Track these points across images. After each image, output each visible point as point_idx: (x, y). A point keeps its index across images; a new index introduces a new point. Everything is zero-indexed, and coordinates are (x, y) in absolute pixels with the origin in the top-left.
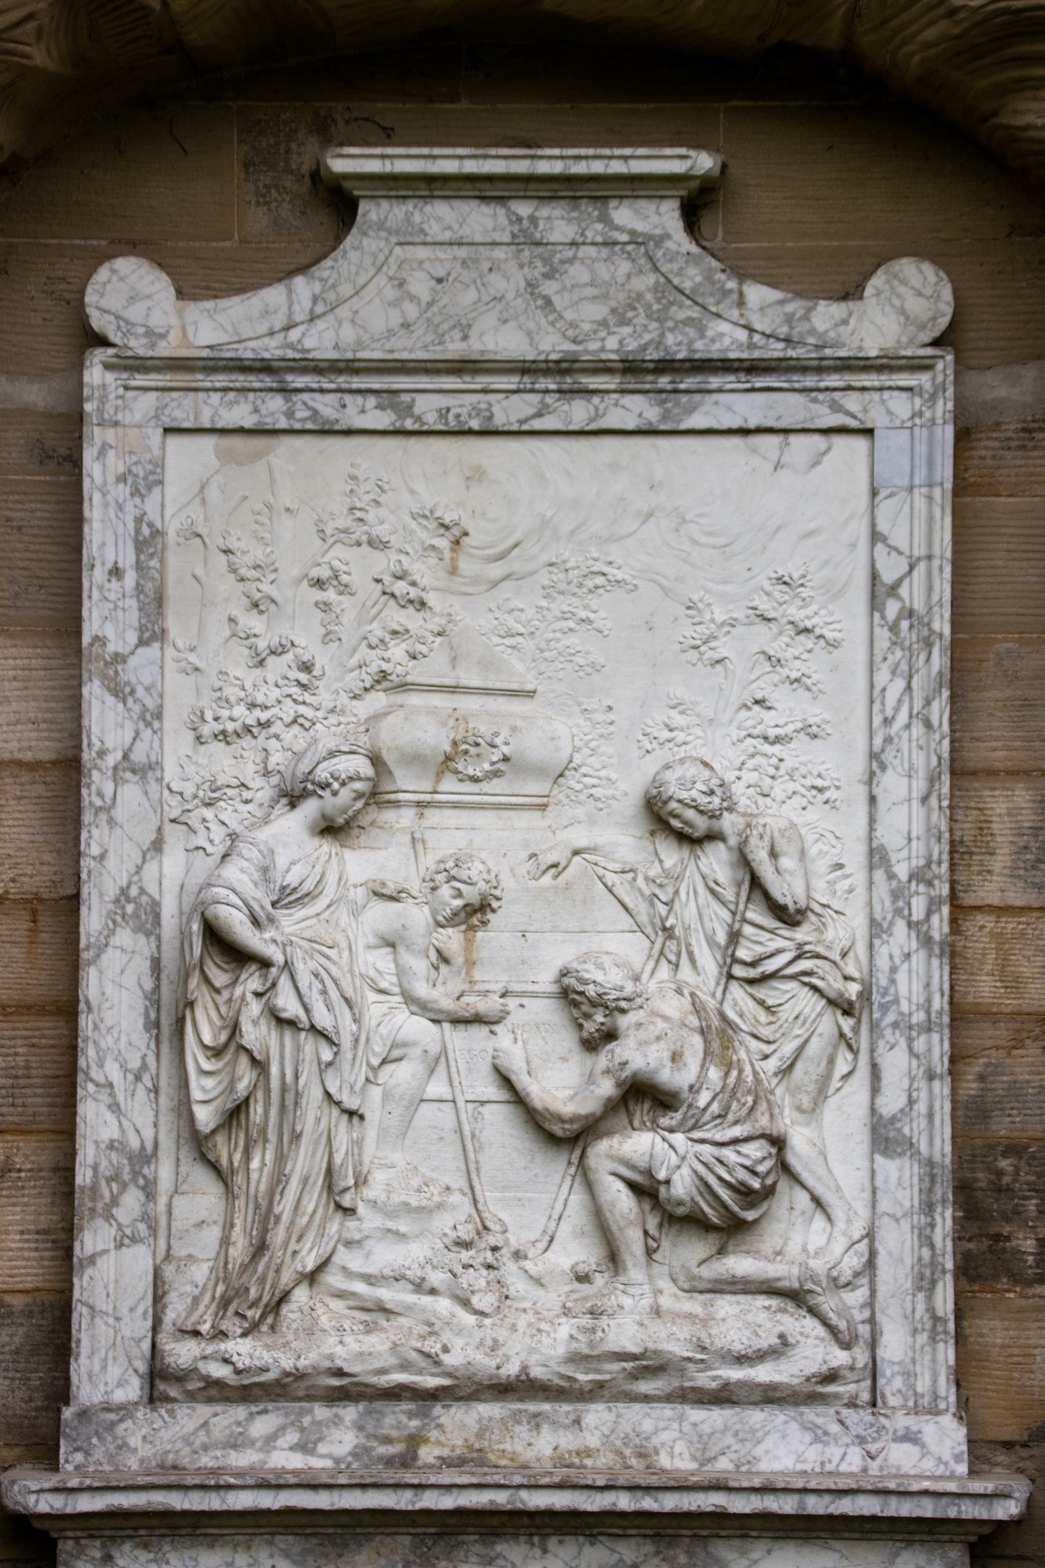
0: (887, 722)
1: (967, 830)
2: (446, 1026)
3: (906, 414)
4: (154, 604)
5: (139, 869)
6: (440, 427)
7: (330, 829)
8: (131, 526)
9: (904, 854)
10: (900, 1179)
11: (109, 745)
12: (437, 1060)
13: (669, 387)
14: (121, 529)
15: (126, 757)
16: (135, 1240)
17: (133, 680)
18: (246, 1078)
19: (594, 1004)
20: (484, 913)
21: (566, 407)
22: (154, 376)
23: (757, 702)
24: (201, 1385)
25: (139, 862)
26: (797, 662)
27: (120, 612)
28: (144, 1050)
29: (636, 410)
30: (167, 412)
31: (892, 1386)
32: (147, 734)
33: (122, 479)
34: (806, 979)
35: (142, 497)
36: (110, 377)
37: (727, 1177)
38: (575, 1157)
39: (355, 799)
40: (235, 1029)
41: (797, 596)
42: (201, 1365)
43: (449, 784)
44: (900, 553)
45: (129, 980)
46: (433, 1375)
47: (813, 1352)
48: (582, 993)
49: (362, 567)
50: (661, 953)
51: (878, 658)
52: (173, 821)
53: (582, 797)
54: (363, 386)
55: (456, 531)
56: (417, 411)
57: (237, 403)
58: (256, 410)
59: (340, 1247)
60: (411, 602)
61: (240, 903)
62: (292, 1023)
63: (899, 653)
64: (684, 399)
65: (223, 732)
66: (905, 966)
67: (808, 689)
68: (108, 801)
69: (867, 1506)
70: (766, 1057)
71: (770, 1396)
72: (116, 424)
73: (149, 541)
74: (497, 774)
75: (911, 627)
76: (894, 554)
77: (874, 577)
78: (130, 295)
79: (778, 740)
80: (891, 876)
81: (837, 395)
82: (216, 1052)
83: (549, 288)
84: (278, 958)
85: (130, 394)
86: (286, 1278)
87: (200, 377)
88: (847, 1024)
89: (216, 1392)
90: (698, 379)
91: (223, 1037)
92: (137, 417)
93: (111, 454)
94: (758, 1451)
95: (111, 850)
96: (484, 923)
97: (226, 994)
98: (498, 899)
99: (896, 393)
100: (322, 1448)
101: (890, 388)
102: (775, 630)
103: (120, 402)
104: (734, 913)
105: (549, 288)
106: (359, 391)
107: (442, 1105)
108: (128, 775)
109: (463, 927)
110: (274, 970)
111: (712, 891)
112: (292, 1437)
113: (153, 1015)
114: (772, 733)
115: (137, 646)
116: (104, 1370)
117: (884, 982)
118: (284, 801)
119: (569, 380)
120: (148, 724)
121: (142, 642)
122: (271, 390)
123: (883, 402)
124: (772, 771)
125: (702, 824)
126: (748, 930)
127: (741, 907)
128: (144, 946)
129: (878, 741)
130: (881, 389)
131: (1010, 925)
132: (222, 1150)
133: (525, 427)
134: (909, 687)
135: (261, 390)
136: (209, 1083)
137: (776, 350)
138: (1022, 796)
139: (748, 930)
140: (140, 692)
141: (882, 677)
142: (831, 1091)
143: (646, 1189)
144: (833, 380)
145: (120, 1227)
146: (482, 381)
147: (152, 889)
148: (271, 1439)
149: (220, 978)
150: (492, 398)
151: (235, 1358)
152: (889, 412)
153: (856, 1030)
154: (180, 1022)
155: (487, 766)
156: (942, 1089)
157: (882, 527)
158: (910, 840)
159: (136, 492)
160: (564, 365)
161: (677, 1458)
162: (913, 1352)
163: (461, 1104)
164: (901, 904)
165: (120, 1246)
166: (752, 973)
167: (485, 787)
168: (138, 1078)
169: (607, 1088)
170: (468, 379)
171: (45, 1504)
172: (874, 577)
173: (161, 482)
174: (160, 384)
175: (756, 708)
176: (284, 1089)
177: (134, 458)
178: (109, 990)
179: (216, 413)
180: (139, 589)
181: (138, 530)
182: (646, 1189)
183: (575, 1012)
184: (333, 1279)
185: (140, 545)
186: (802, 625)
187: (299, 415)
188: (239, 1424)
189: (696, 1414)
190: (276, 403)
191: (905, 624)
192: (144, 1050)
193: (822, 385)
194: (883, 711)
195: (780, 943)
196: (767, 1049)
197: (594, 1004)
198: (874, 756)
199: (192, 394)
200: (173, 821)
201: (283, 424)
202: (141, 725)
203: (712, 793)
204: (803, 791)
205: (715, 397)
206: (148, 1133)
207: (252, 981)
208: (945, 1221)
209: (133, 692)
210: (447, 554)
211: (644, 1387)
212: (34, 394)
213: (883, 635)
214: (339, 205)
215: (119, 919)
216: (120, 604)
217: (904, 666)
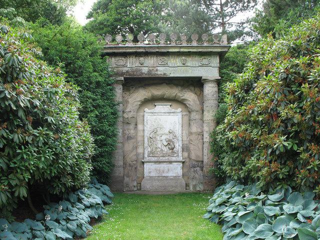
78: (146, 110)
116: (146, 156)
143: (169, 148)
161: (170, 159)
162: (180, 154)
182: (169, 148)
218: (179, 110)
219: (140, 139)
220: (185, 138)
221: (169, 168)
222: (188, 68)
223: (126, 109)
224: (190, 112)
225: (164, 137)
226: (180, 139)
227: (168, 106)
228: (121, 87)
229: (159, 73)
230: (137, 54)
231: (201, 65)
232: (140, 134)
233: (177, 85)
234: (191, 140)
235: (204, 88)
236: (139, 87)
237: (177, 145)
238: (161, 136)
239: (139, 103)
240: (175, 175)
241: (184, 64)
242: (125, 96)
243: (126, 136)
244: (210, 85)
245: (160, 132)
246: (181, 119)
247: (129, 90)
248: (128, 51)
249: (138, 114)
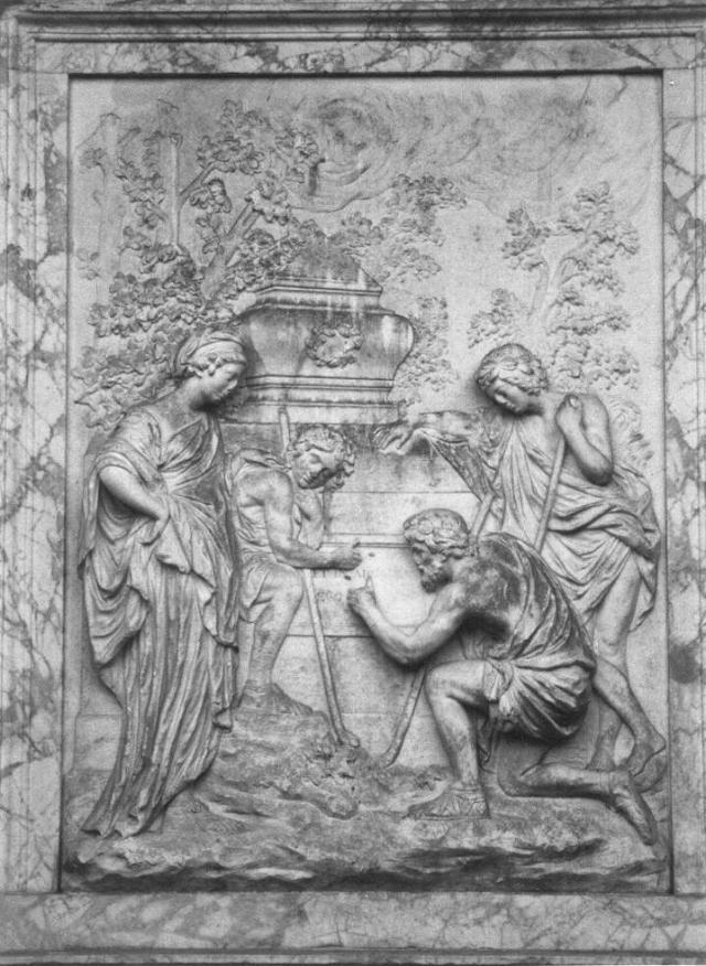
0: (679, 314)
2: (307, 572)
3: (690, 57)
5: (48, 441)
6: (301, 71)
8: (41, 156)
9: (694, 426)
11: (22, 336)
12: (300, 601)
13: (492, 35)
14: (32, 157)
15: (36, 347)
16: (45, 754)
17: (43, 283)
19: (434, 551)
20: (339, 477)
21: (405, 53)
22: (60, 30)
23: (568, 299)
24: (100, 877)
25: (48, 435)
26: (601, 266)
27: (31, 227)
28: (52, 595)
30: (72, 59)
32: (54, 328)
33: (34, 115)
34: (611, 530)
35: (51, 131)
36: (24, 30)
37: (548, 698)
38: (418, 684)
39: (229, 380)
40: (126, 573)
41: (599, 211)
42: (97, 860)
43: (308, 369)
44: (686, 173)
45: (40, 535)
46: (296, 869)
47: (622, 849)
48: (422, 542)
50: (490, 510)
51: (669, 259)
52: (76, 402)
53: (422, 379)
54: (235, 36)
55: (314, 158)
56: (280, 57)
57: (129, 52)
58: (146, 58)
59: (218, 759)
60: (276, 217)
61: (129, 466)
62: (173, 568)
63: (687, 257)
64: (505, 45)
65: (118, 326)
66: (696, 519)
67: (611, 288)
68: (21, 384)
70: (579, 597)
72: (28, 70)
74: (348, 360)
75: (696, 235)
76: (681, 174)
77: (666, 192)
79: (585, 331)
80: (683, 444)
81: (632, 41)
82: (112, 595)
84: (162, 513)
85: (40, 45)
86: (171, 788)
87: (99, 30)
88: (647, 567)
90: (516, 28)
91: (117, 582)
92: (47, 65)
93: (24, 94)
94: (576, 932)
95: (24, 425)
96: (340, 485)
97: (119, 545)
98: (352, 465)
99: (681, 39)
100: (204, 931)
101: (677, 35)
102: (582, 240)
103: (31, 51)
104: (550, 476)
106: (231, 41)
107: (305, 640)
108: (39, 363)
109: (322, 489)
110: (159, 524)
111: (531, 457)
112: (177, 922)
113: (60, 564)
114: (581, 325)
115: (46, 255)
117: (677, 533)
118: (171, 382)
119: (407, 29)
120: (54, 320)
121: (51, 252)
122: (158, 40)
123: (670, 46)
124: (581, 357)
125: (523, 398)
126: (563, 490)
127: (557, 470)
128: (53, 508)
129: (671, 329)
130: (669, 36)
132: (116, 677)
133: (372, 70)
134: (695, 285)
135: (149, 41)
136: (106, 620)
139: (563, 490)
140: (49, 293)
141: (672, 278)
142: (632, 627)
143: (477, 708)
144: (629, 28)
145: (32, 744)
146: (336, 30)
147: (60, 458)
148: (157, 925)
149: (114, 531)
150: (344, 45)
151: (128, 855)
152: (675, 54)
153: (654, 574)
154: (81, 567)
155: (341, 354)
157: (670, 150)
158: (698, 413)
159: (46, 127)
160: (404, 15)
163: (320, 639)
164: (691, 468)
165: (30, 758)
166: (568, 526)
167: (338, 371)
168: (47, 616)
169: (444, 622)
170: (323, 29)
172: (666, 192)
173: (68, 120)
174: (67, 36)
175: (566, 304)
176: (169, 623)
177: (44, 99)
178: (22, 544)
179: (112, 61)
180: (48, 207)
181: (47, 158)
183: (417, 558)
185: (49, 171)
186: (604, 235)
187: (181, 61)
188: (132, 910)
190: (163, 51)
191: (691, 233)
192: (52, 595)
193: (619, 32)
194: (674, 305)
195: (588, 500)
196: (581, 590)
197: (434, 551)
198: (666, 343)
199: (91, 45)
200: (76, 402)
201: (168, 69)
202: (49, 320)
203: (532, 373)
204: (607, 373)
205: (529, 44)
206: (56, 663)
207: (141, 531)
209: (42, 294)
210: (307, 178)
213: (673, 245)
215: (30, 483)
216: (32, 219)
217: (691, 268)
238: (327, 479)
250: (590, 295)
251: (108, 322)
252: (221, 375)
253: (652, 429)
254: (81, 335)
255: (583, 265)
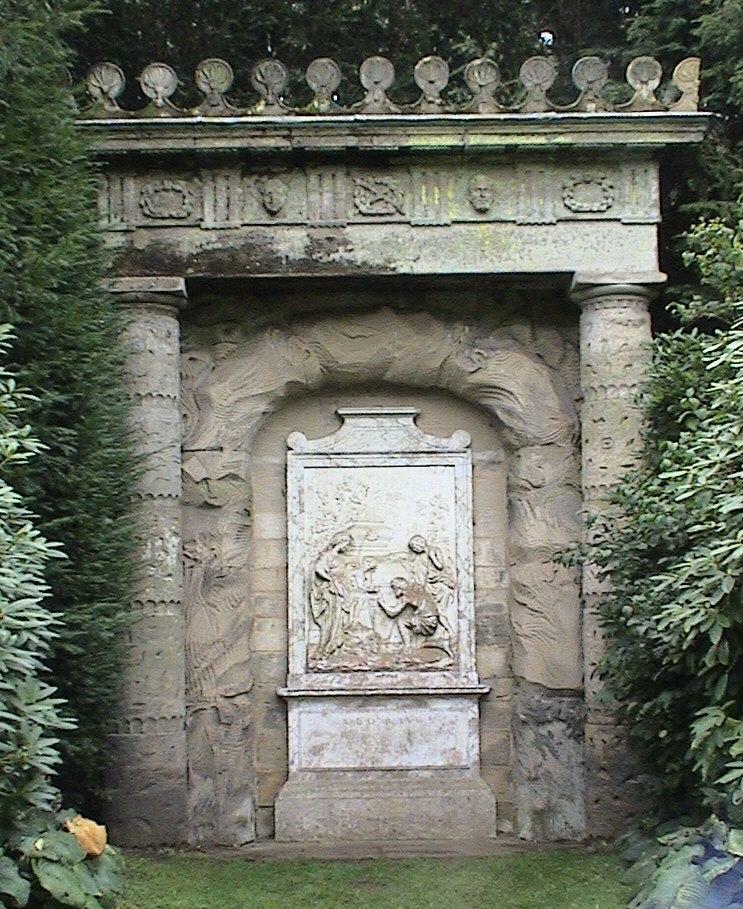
1: (476, 549)
4: (301, 504)
7: (340, 552)
10: (464, 624)
18: (325, 605)
29: (405, 461)
31: (462, 666)
49: (347, 495)
69: (457, 691)
71: (436, 669)
73: (300, 492)
78: (297, 439)
83: (385, 436)
89: (319, 671)
105: (385, 436)
116: (297, 666)
131: (485, 570)
137: (434, 449)
138: (488, 542)
141: (458, 517)
146: (372, 456)
156: (472, 604)
162: (466, 660)
169: (401, 606)
171: (286, 694)
182: (410, 627)
184: (344, 647)
189: (422, 674)
190: (328, 461)
208: (473, 631)
211: (410, 668)
212: (277, 461)
214: (341, 419)
218: (459, 439)
219: (267, 582)
220: (487, 579)
221: (415, 726)
222: (503, 228)
223: (195, 436)
224: (511, 449)
225: (383, 576)
226: (466, 581)
227: (402, 420)
228: (172, 325)
229: (359, 256)
230: (254, 164)
231: (570, 215)
232: (269, 558)
233: (448, 317)
234: (522, 587)
235: (585, 330)
236: (261, 328)
237: (449, 614)
239: (263, 407)
240: (440, 763)
241: (482, 211)
242: (194, 369)
243: (198, 571)
244: (613, 314)
245: (362, 552)
246: (466, 485)
247: (211, 343)
248: (205, 144)
249: (257, 460)
250: (436, 522)
251: (314, 530)
252: (345, 544)
253: (453, 556)
254: (307, 534)
255: (435, 514)
